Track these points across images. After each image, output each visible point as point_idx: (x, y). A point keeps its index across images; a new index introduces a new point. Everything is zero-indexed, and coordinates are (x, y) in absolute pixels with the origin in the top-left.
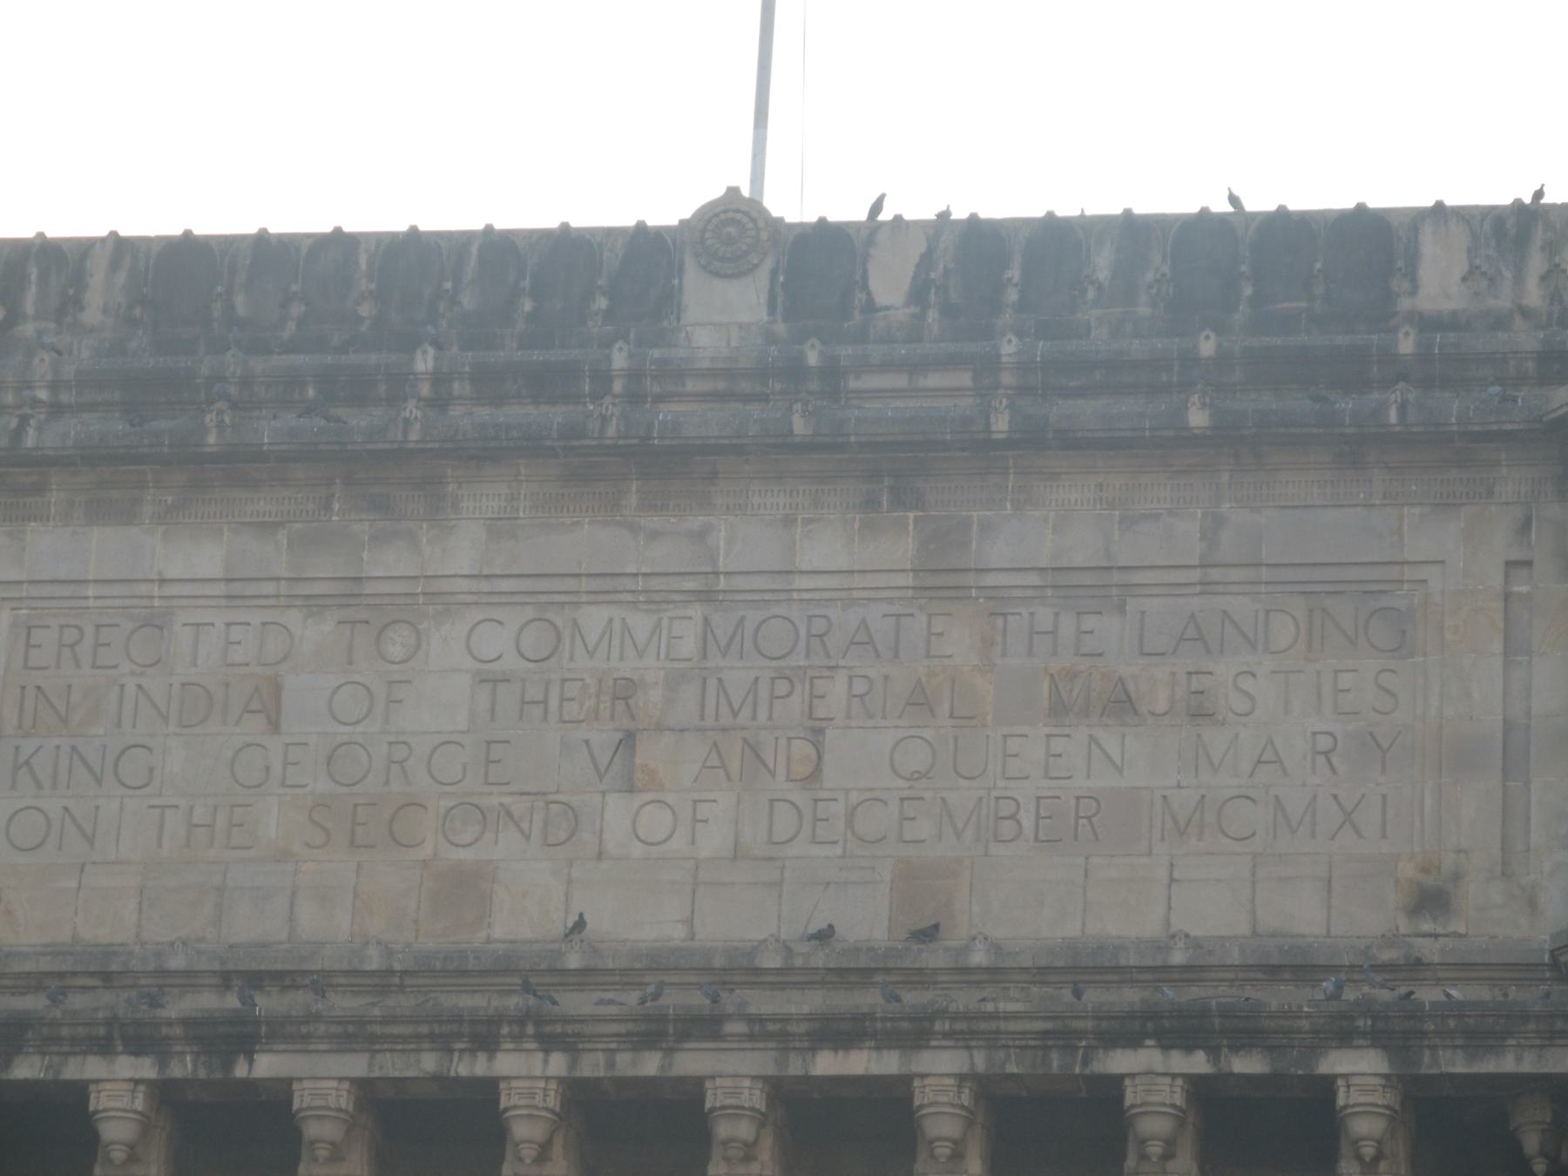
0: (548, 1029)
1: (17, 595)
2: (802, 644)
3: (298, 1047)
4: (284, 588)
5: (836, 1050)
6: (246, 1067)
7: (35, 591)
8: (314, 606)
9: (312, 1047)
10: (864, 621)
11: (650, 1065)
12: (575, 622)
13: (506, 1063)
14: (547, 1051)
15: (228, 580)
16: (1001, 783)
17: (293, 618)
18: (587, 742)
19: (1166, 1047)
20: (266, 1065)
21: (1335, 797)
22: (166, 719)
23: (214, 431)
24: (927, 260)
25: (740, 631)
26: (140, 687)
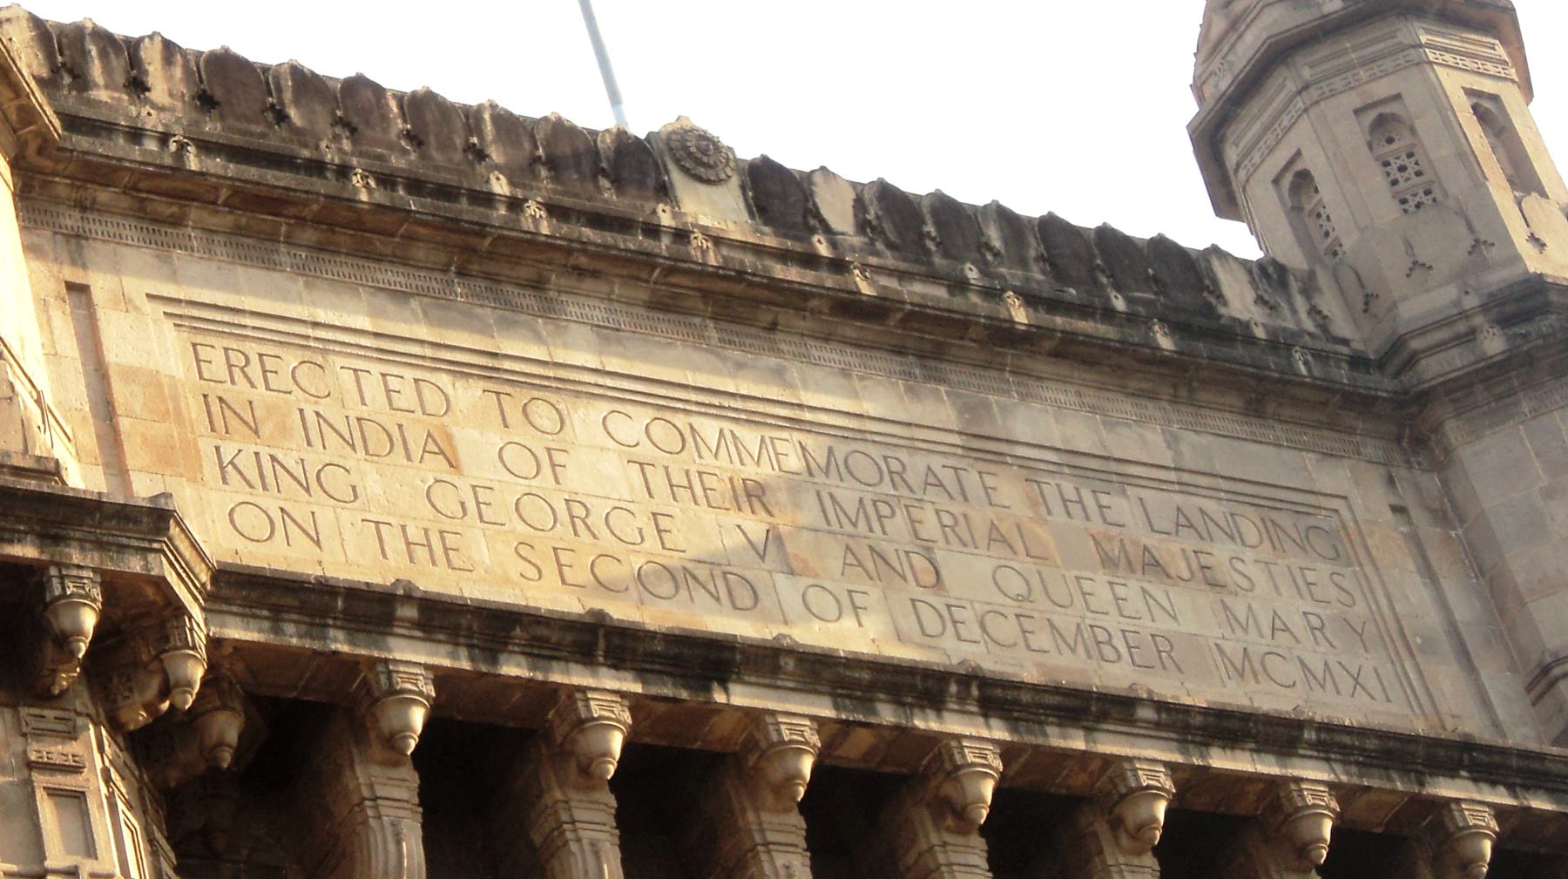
0: (989, 692)
2: (887, 477)
3: (766, 681)
4: (429, 352)
5: (1223, 748)
7: (195, 312)
8: (460, 371)
9: (779, 683)
10: (929, 468)
11: (1077, 742)
13: (953, 724)
14: (986, 716)
16: (1090, 615)
17: (444, 380)
18: (739, 526)
20: (740, 696)
21: (1340, 663)
23: (364, 190)
24: (859, 204)
26: (318, 414)
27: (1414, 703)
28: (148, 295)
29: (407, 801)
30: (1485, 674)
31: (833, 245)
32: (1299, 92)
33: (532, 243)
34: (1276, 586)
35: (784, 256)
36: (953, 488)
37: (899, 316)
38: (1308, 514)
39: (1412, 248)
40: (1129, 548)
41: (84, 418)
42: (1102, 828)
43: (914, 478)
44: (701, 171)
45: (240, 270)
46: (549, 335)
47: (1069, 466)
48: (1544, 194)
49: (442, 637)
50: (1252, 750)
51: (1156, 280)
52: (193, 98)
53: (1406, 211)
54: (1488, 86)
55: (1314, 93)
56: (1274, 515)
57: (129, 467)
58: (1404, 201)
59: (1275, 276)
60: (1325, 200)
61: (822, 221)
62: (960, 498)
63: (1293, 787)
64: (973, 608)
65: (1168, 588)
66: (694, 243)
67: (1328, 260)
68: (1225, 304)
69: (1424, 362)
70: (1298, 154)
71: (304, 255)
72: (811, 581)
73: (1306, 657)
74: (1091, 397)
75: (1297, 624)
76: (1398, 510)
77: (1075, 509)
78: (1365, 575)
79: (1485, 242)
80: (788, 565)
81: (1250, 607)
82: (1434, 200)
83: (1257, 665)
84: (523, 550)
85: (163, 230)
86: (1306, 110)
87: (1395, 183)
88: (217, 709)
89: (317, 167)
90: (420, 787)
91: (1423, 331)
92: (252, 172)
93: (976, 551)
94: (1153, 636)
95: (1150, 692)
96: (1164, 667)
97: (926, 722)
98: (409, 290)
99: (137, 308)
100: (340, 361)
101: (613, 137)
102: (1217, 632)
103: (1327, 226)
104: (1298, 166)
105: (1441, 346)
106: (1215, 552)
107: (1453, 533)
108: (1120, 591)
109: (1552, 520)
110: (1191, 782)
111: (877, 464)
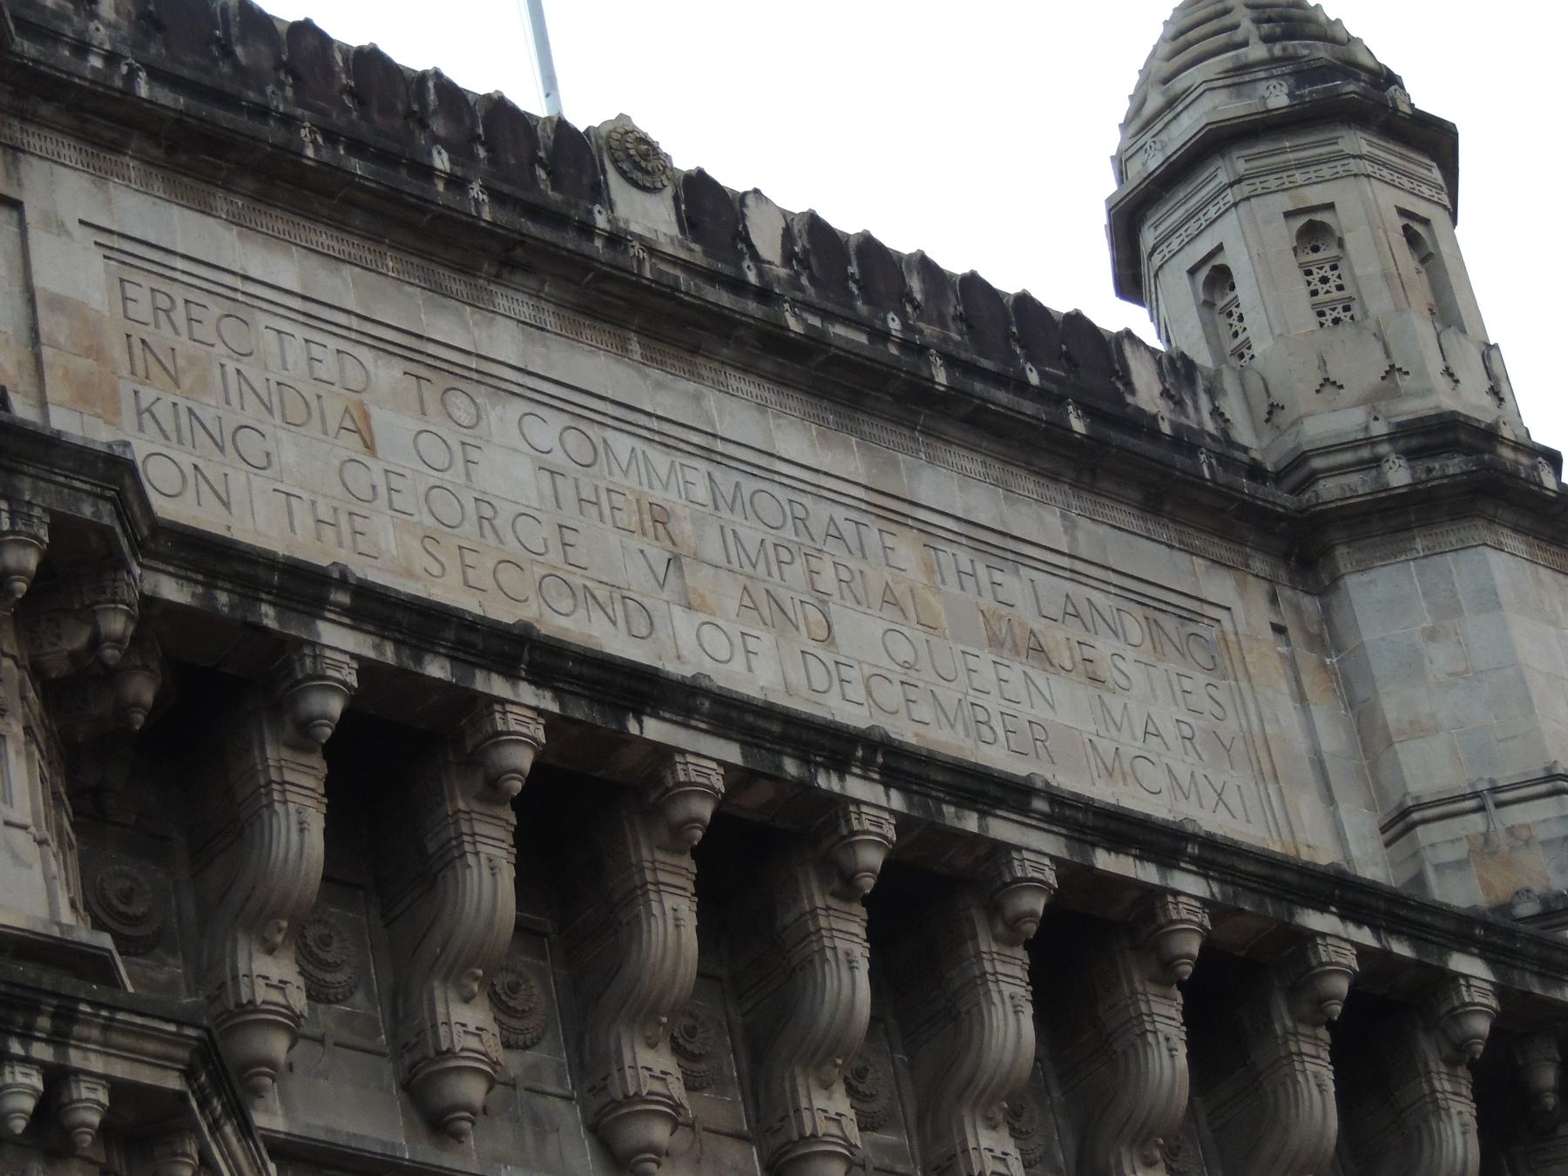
1: (110, 244)
3: (680, 719)
4: (355, 323)
6: (637, 726)
8: (382, 348)
9: (693, 723)
10: (832, 519)
11: (971, 823)
12: (605, 441)
13: (856, 787)
14: (887, 786)
15: (304, 298)
16: (972, 692)
17: (365, 354)
19: (1343, 917)
20: (655, 729)
22: (270, 410)
23: (311, 145)
24: (788, 235)
25: (739, 495)
26: (238, 372)
27: (1272, 828)
28: (81, 222)
29: (313, 790)
30: (1343, 809)
31: (760, 274)
32: (1231, 185)
33: (470, 226)
34: (1153, 690)
35: (712, 277)
36: (854, 544)
37: (822, 358)
38: (1190, 620)
39: (1325, 363)
40: (1017, 630)
41: (7, 341)
42: (977, 916)
43: (817, 528)
44: (637, 175)
45: (175, 209)
46: (475, 324)
47: (967, 536)
48: (1464, 331)
49: (371, 628)
50: (1135, 857)
51: (1068, 357)
52: (138, 18)
53: (1322, 325)
54: (1422, 209)
55: (1244, 189)
56: (1158, 615)
57: (49, 400)
58: (1321, 314)
59: (1183, 371)
60: (1240, 300)
61: (751, 246)
62: (858, 554)
63: (1170, 899)
64: (861, 669)
65: (1052, 677)
66: (631, 251)
67: (1234, 361)
68: (1133, 392)
69: (1322, 482)
70: (1220, 248)
71: (240, 203)
72: (706, 618)
73: (1175, 766)
74: (996, 470)
75: (1170, 732)
76: (1279, 629)
77: (969, 582)
78: (1240, 690)
79: (1400, 369)
80: (687, 598)
81: (1125, 706)
82: (1352, 318)
83: (1127, 768)
84: (428, 543)
85: (102, 155)
86: (1235, 205)
87: (1314, 293)
88: (136, 667)
89: (262, 112)
90: (327, 777)
91: (1328, 450)
92: (205, 110)
93: (869, 611)
94: (1030, 722)
95: (1047, 784)
96: (1038, 757)
97: (827, 781)
98: (341, 256)
99: (68, 233)
100: (263, 320)
101: (554, 126)
102: (1092, 728)
103: (1238, 326)
104: (1218, 261)
105: (1342, 469)
106: (1098, 645)
107: (1328, 661)
108: (1004, 673)
109: (1431, 662)
110: (1076, 876)
111: (782, 507)
